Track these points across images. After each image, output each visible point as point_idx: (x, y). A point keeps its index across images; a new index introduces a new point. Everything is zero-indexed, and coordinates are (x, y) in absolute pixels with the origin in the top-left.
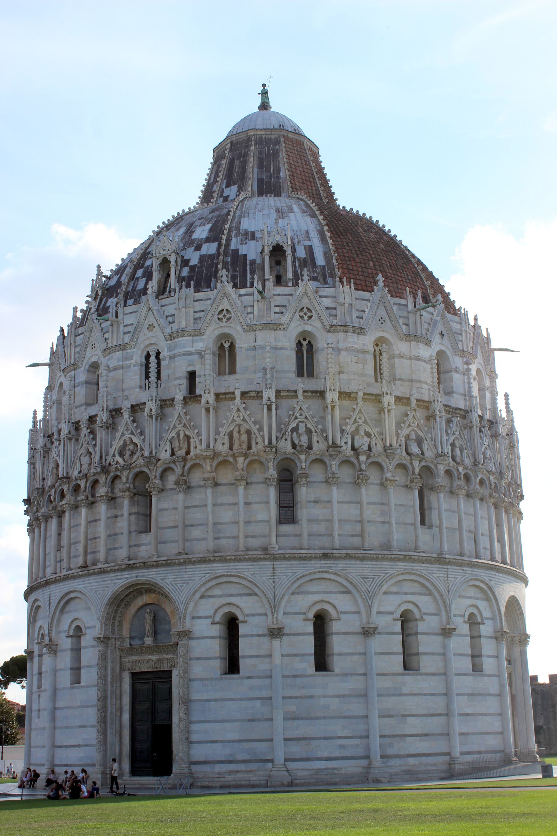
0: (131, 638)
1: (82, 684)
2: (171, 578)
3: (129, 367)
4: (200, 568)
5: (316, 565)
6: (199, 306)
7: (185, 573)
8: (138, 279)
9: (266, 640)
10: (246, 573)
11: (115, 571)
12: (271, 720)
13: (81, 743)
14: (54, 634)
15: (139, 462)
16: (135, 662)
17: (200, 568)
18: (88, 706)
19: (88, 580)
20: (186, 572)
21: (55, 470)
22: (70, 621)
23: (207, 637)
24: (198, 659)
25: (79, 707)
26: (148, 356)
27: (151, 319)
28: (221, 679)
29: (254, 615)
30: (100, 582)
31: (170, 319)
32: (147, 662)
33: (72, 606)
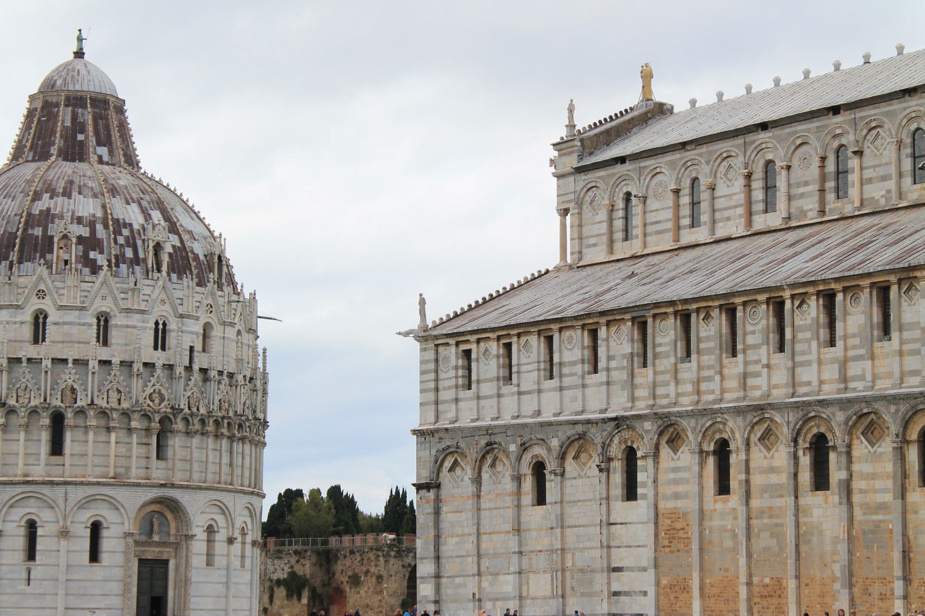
0: (140, 534)
1: (104, 564)
3: (146, 328)
5: (248, 498)
6: (198, 297)
8: (121, 245)
9: (226, 544)
11: (146, 486)
12: (226, 597)
13: (103, 606)
14: (69, 523)
15: (164, 408)
16: (144, 551)
21: (68, 393)
22: (89, 515)
26: (157, 323)
27: (163, 296)
31: (179, 301)
32: (151, 553)
33: (93, 505)
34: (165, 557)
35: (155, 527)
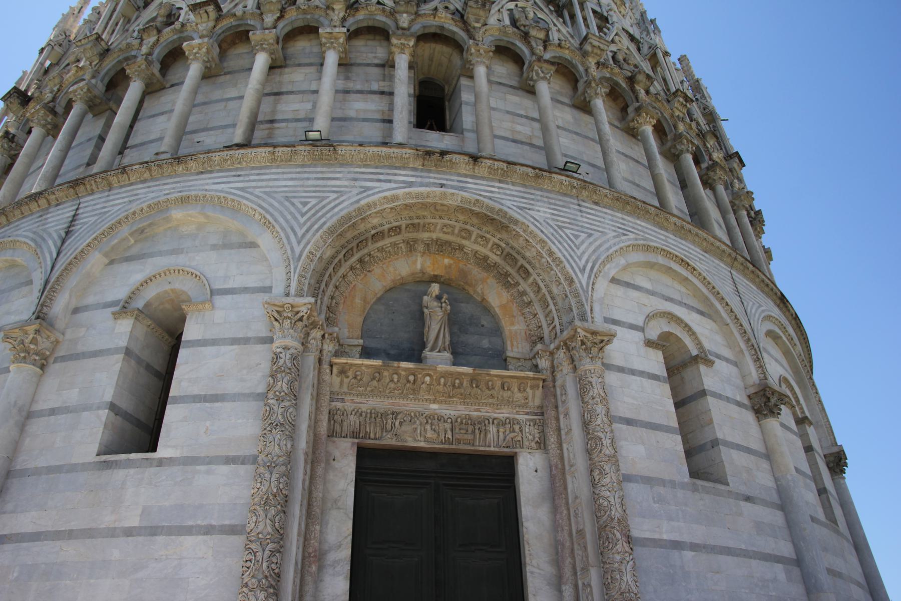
1: (163, 451)
2: (545, 212)
4: (612, 215)
7: (579, 214)
10: (698, 264)
16: (377, 416)
17: (612, 215)
18: (188, 531)
19: (258, 174)
20: (581, 211)
23: (642, 374)
24: (629, 422)
25: (129, 532)
28: (695, 489)
29: (719, 357)
30: (308, 179)
34: (492, 442)
35: (435, 326)
